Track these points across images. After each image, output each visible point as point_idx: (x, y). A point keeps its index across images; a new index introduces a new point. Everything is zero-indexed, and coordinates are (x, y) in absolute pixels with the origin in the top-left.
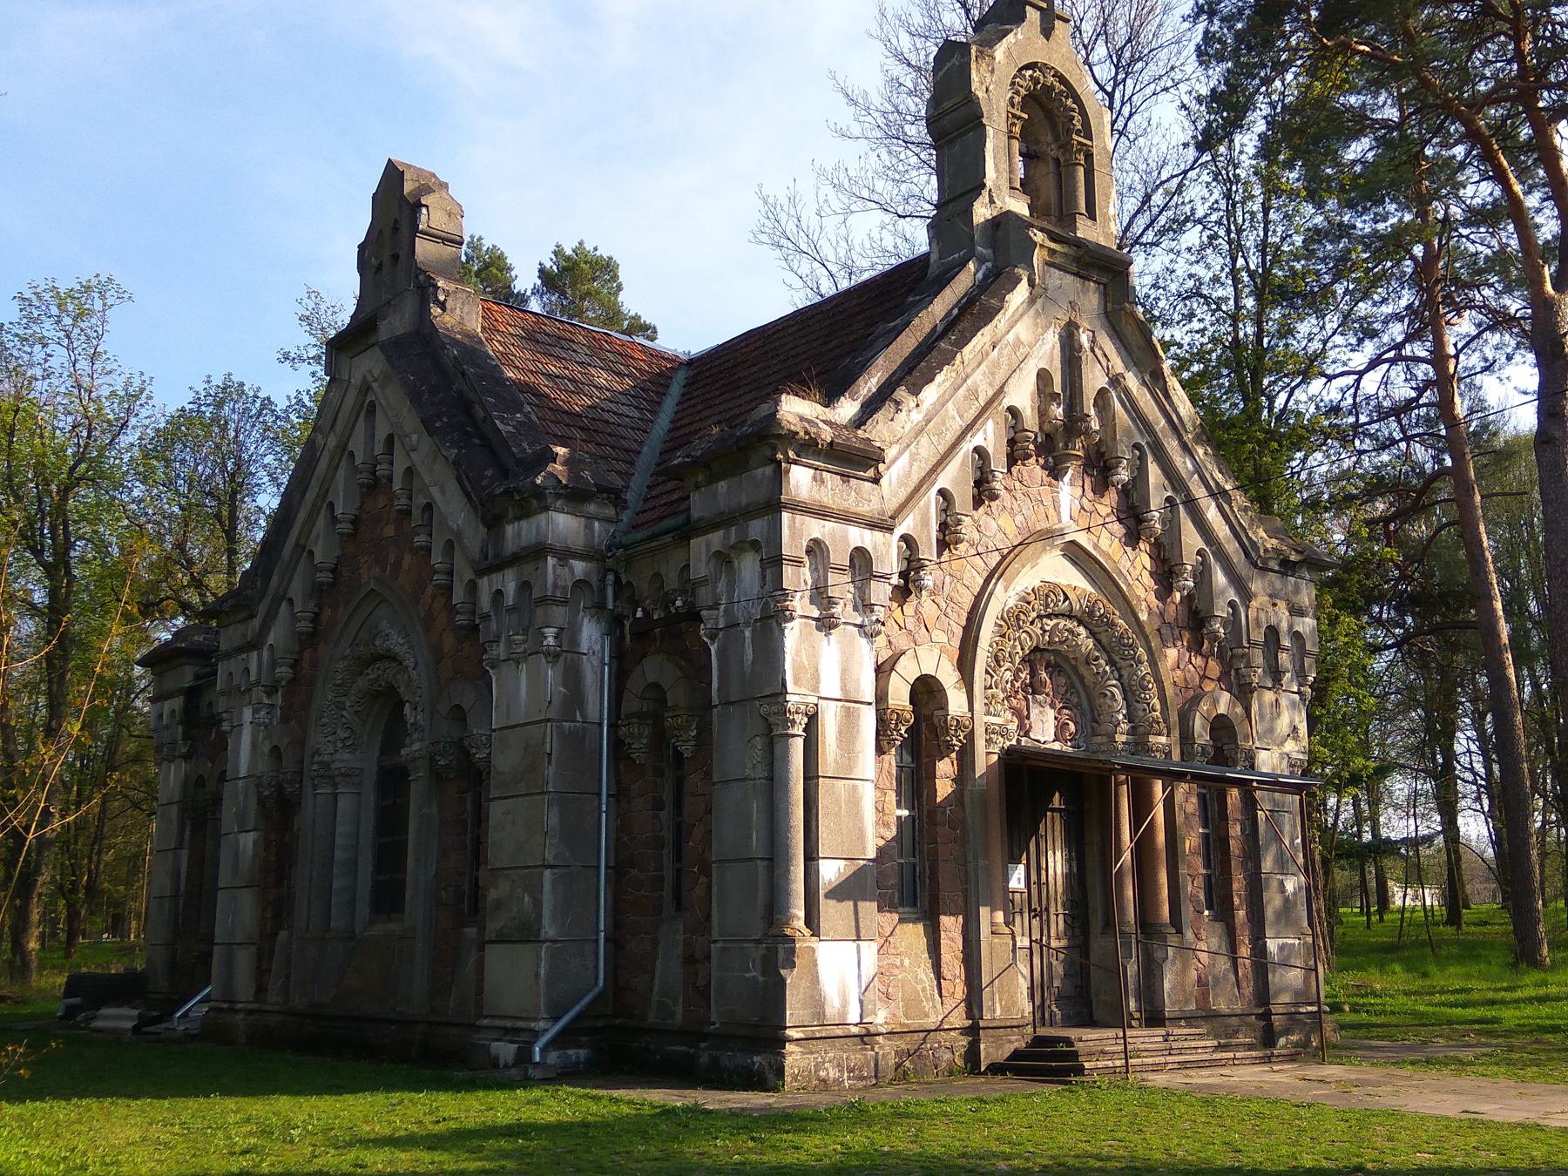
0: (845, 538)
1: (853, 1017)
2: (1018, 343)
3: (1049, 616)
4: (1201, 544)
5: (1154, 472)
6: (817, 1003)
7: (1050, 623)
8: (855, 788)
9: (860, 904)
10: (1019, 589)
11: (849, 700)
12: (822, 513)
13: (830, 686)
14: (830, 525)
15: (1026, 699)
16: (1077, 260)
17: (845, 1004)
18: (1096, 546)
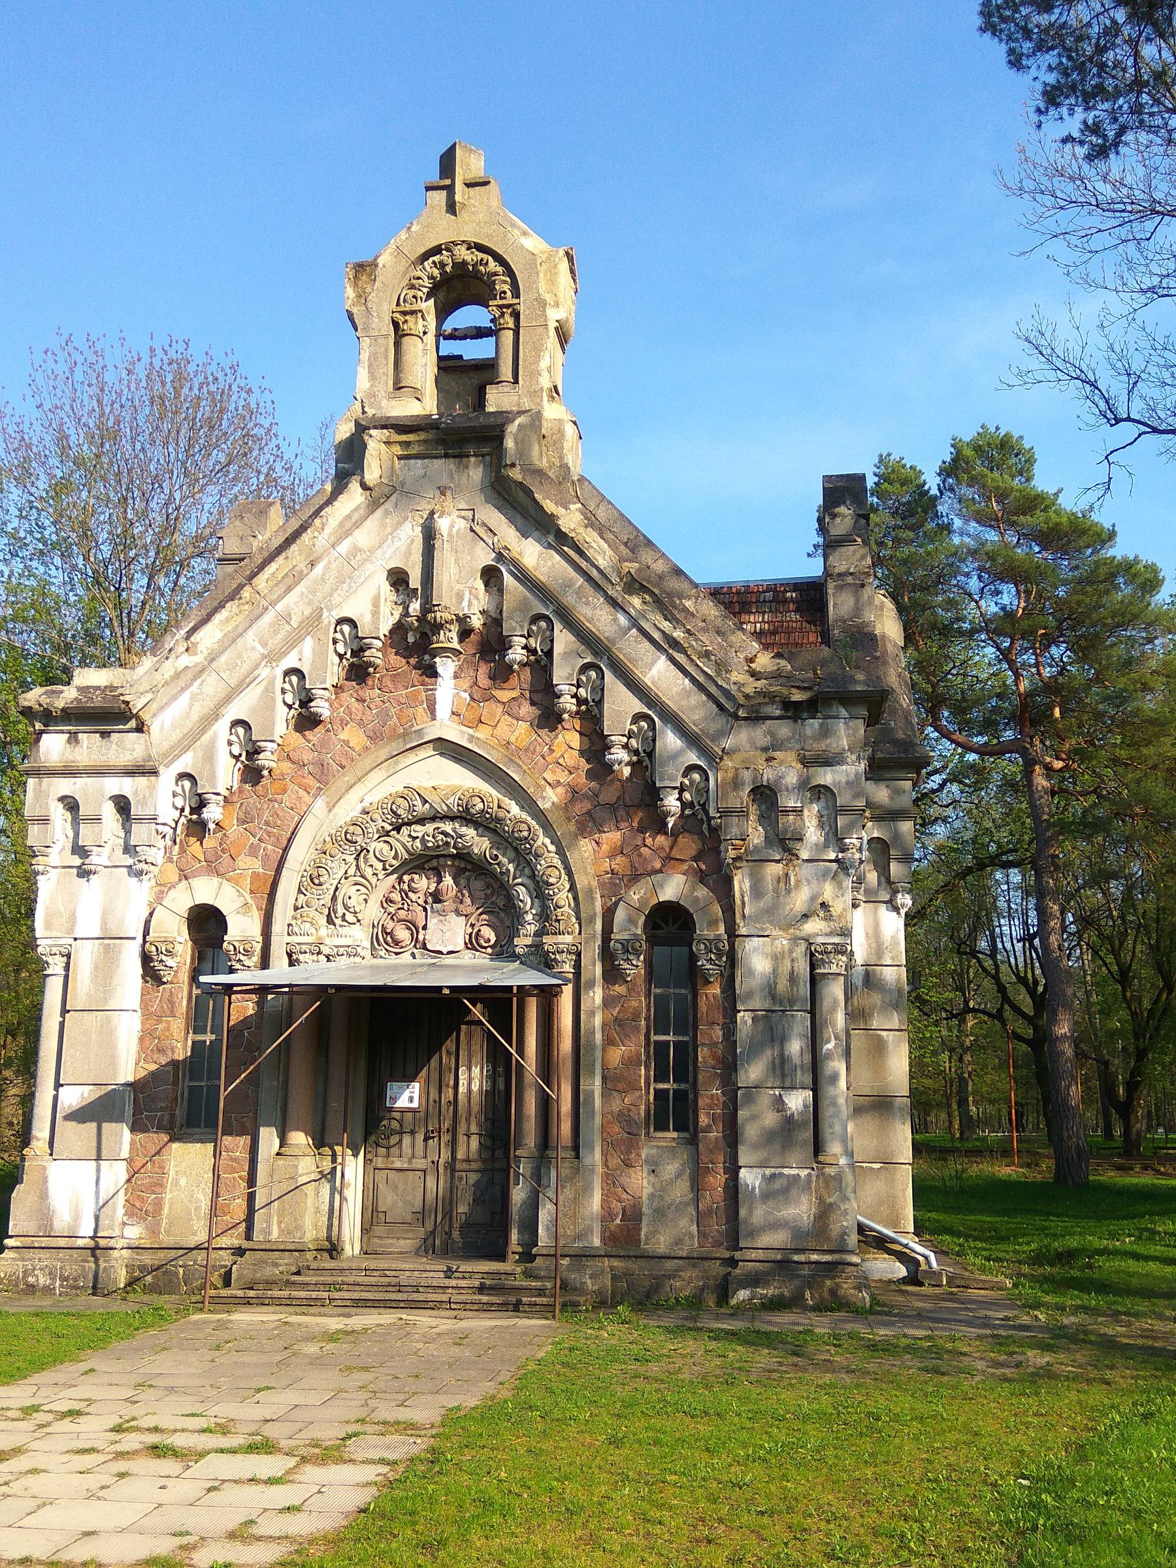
0: (101, 791)
1: (87, 1229)
2: (356, 550)
3: (421, 821)
4: (638, 707)
5: (563, 640)
6: (45, 1215)
7: (419, 830)
8: (109, 1020)
9: (105, 1125)
10: (369, 799)
11: (110, 939)
12: (69, 772)
13: (88, 925)
14: (81, 782)
15: (425, 910)
16: (441, 441)
17: (77, 1217)
18: (471, 738)
